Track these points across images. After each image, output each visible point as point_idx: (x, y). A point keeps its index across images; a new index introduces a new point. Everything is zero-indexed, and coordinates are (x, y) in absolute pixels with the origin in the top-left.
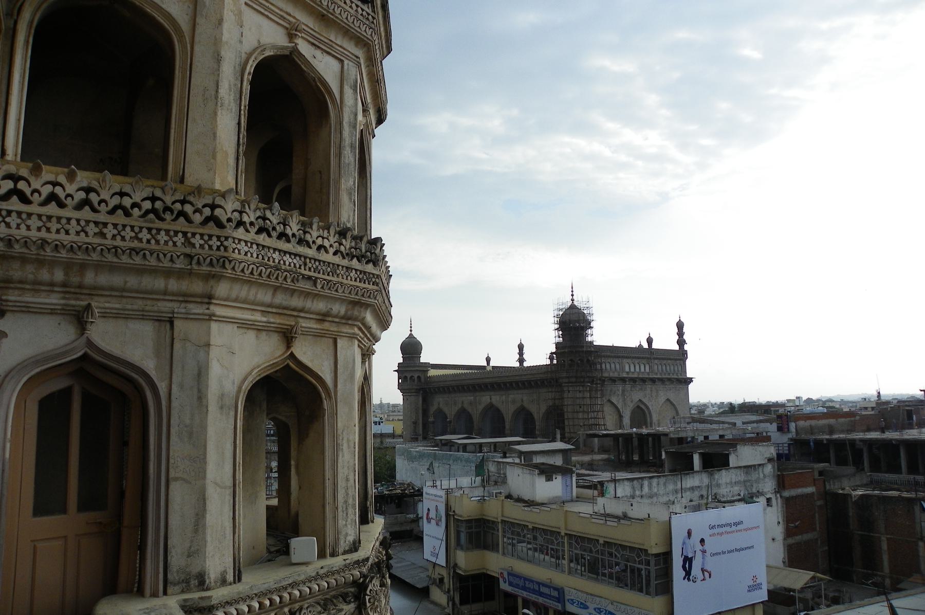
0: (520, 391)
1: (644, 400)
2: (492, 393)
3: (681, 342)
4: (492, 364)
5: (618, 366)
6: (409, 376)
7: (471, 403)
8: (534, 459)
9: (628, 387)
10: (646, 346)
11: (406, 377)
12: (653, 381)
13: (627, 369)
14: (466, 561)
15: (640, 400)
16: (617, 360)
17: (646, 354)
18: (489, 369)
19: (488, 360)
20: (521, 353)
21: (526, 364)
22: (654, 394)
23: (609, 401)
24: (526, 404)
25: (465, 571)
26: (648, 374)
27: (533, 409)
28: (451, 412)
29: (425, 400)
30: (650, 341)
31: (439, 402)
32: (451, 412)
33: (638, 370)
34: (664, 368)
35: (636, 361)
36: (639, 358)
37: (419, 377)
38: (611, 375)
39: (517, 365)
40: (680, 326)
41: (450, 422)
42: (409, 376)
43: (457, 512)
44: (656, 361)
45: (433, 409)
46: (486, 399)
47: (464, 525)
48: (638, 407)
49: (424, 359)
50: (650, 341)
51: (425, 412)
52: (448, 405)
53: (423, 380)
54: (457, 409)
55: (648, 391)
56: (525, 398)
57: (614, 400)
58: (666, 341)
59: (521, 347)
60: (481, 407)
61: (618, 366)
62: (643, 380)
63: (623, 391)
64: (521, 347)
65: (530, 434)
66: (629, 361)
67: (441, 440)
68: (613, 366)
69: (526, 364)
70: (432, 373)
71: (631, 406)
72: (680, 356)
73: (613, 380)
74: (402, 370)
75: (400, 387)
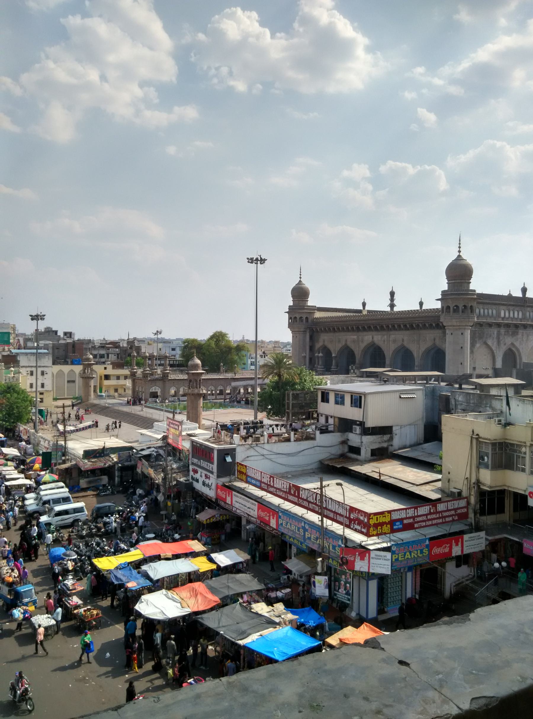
0: (400, 332)
1: (515, 343)
2: (374, 333)
4: (367, 308)
5: (494, 312)
6: (298, 316)
7: (354, 341)
8: (491, 391)
9: (503, 331)
10: (520, 295)
11: (295, 318)
12: (525, 327)
13: (502, 315)
14: (488, 478)
15: (512, 344)
16: (494, 307)
18: (365, 313)
19: (364, 304)
20: (392, 299)
21: (396, 309)
22: (525, 339)
23: (486, 343)
24: (405, 344)
25: (490, 487)
26: (521, 320)
28: (335, 349)
29: (311, 338)
30: (524, 290)
31: (324, 339)
32: (335, 349)
33: (512, 315)
35: (511, 308)
36: (513, 305)
37: (307, 318)
38: (489, 320)
39: (388, 309)
41: (336, 357)
42: (298, 316)
43: (481, 435)
44: (529, 309)
45: (318, 346)
46: (368, 338)
47: (490, 447)
48: (510, 349)
49: (311, 302)
50: (524, 290)
51: (312, 348)
52: (334, 343)
53: (310, 320)
54: (340, 346)
55: (520, 336)
56: (406, 338)
57: (490, 342)
59: (392, 294)
60: (363, 346)
61: (494, 312)
62: (516, 326)
63: (499, 334)
64: (392, 294)
66: (504, 307)
67: (366, 372)
68: (486, 311)
69: (396, 309)
70: (318, 315)
71: (504, 348)
73: (490, 325)
75: (290, 326)
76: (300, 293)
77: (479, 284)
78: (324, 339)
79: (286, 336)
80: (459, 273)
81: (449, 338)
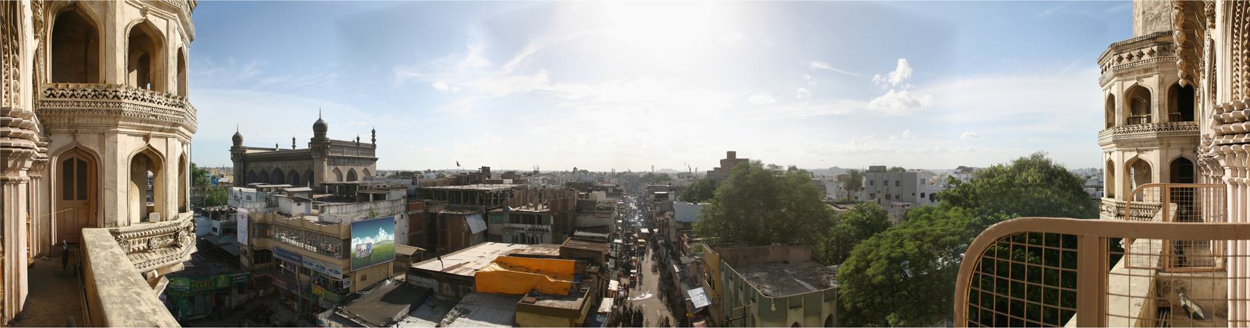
3: (374, 140)
17: (357, 145)
27: (298, 170)
31: (252, 166)
32: (258, 171)
34: (364, 153)
40: (373, 132)
46: (275, 165)
49: (244, 144)
51: (245, 171)
58: (366, 139)
65: (296, 185)
70: (248, 152)
72: (373, 147)
74: (233, 149)
76: (237, 139)
77: (331, 135)
78: (252, 166)
79: (231, 164)
80: (320, 128)
81: (316, 165)
